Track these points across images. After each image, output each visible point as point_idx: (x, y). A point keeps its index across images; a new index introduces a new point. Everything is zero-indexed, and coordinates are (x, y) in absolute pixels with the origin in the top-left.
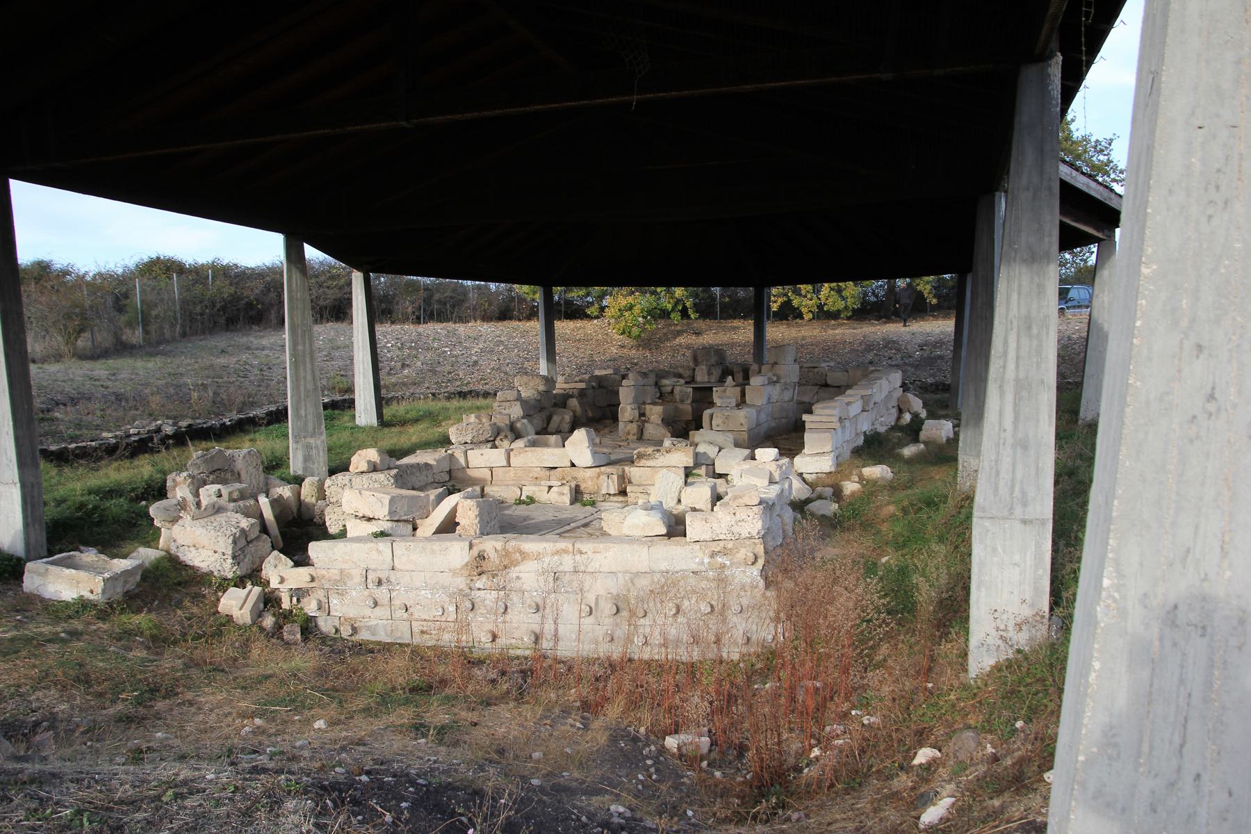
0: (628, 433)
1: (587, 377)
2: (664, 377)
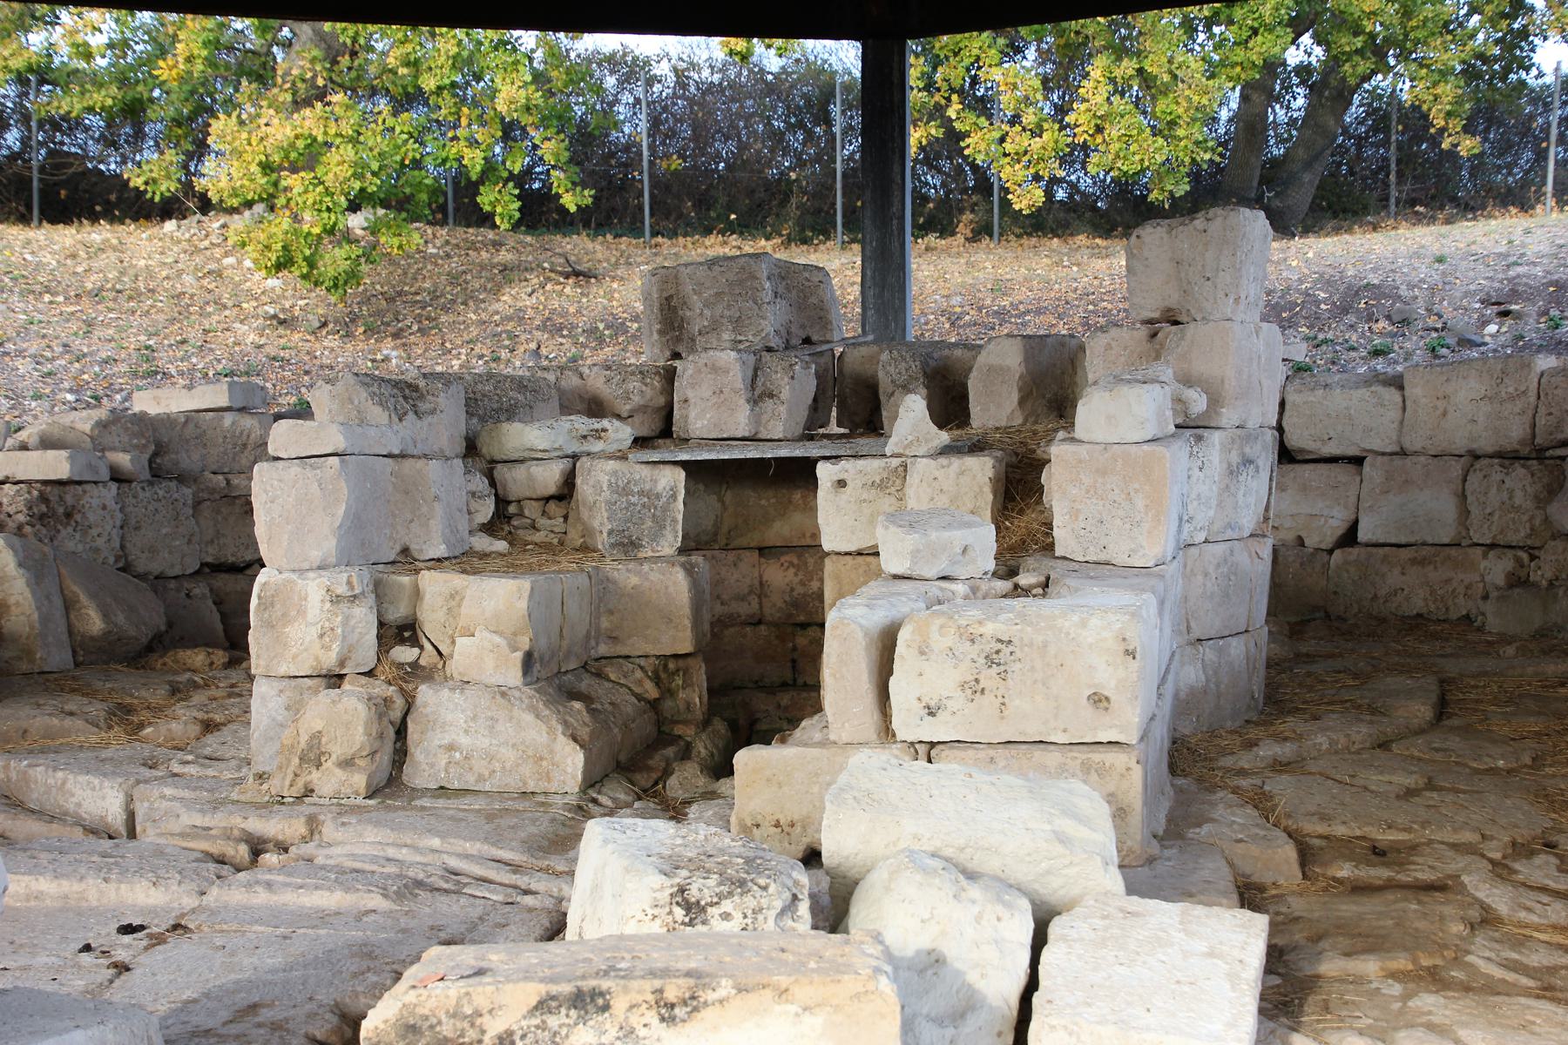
0: (313, 756)
1: (84, 421)
2: (511, 413)
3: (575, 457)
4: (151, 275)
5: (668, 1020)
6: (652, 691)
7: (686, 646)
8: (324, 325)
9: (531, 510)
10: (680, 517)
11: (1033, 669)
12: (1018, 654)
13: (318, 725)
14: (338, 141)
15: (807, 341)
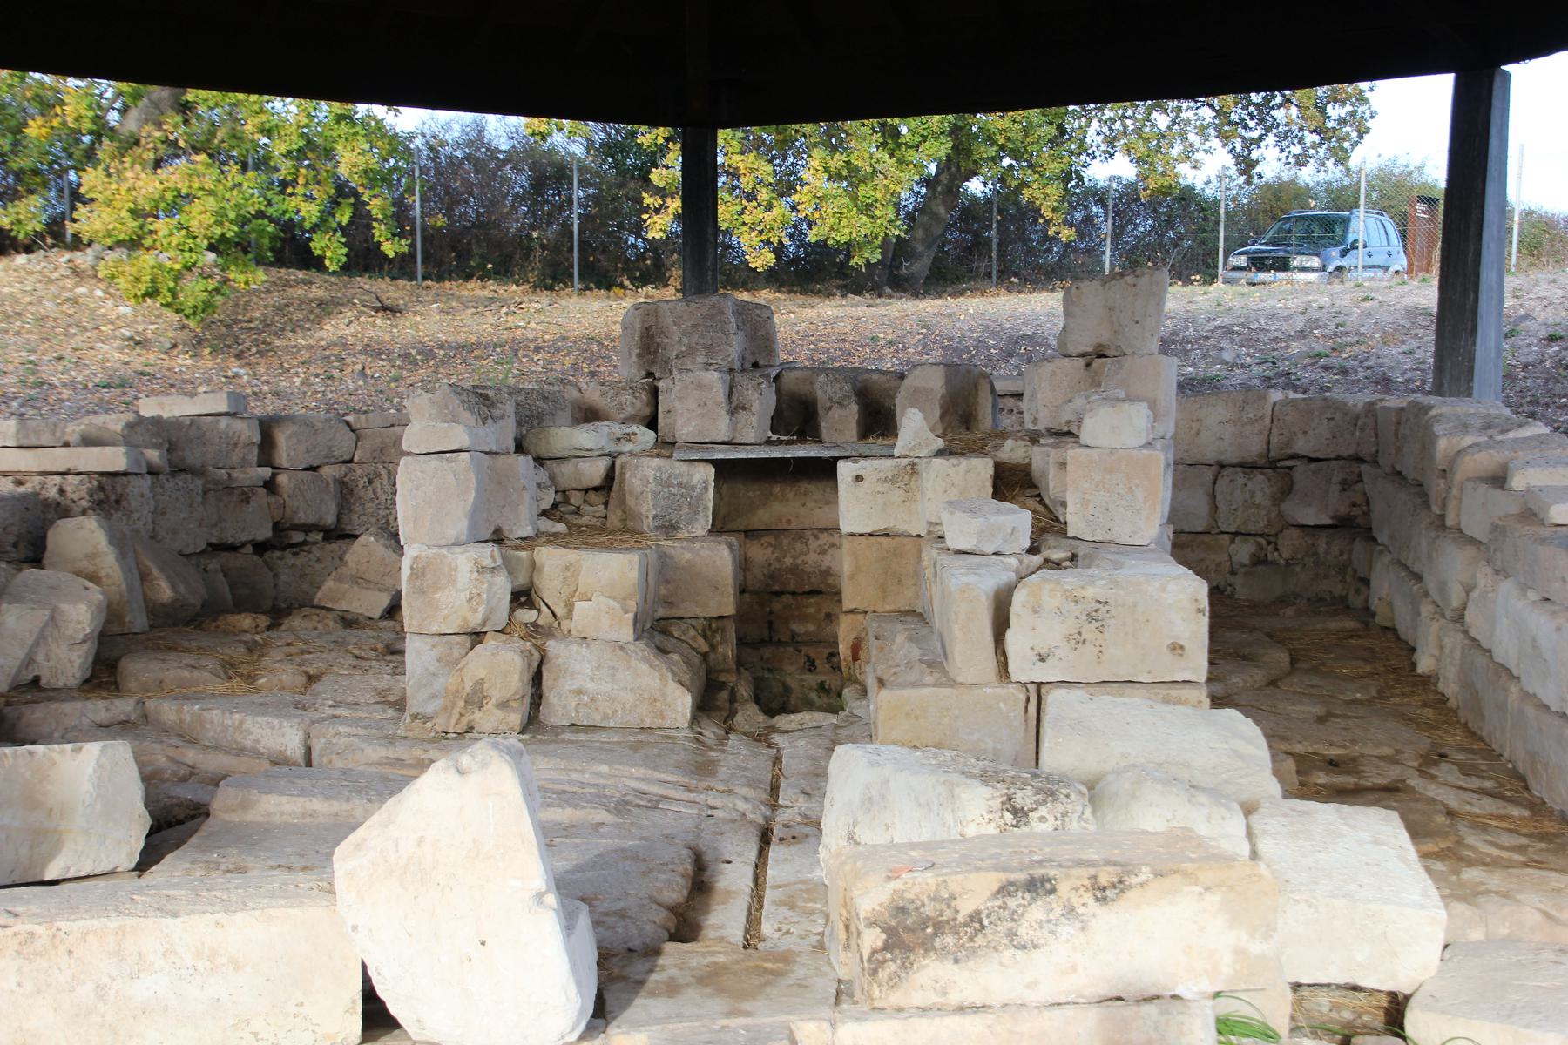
0: (476, 699)
3: (613, 456)
4: (16, 302)
5: (1103, 900)
6: (705, 647)
7: (730, 610)
8: (175, 346)
9: (576, 499)
10: (711, 505)
11: (1124, 624)
12: (1113, 612)
13: (481, 674)
14: (200, 193)
15: (755, 365)
